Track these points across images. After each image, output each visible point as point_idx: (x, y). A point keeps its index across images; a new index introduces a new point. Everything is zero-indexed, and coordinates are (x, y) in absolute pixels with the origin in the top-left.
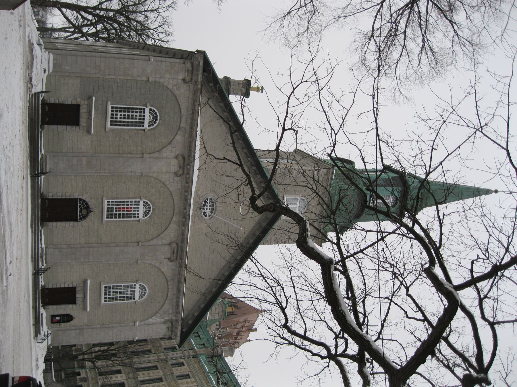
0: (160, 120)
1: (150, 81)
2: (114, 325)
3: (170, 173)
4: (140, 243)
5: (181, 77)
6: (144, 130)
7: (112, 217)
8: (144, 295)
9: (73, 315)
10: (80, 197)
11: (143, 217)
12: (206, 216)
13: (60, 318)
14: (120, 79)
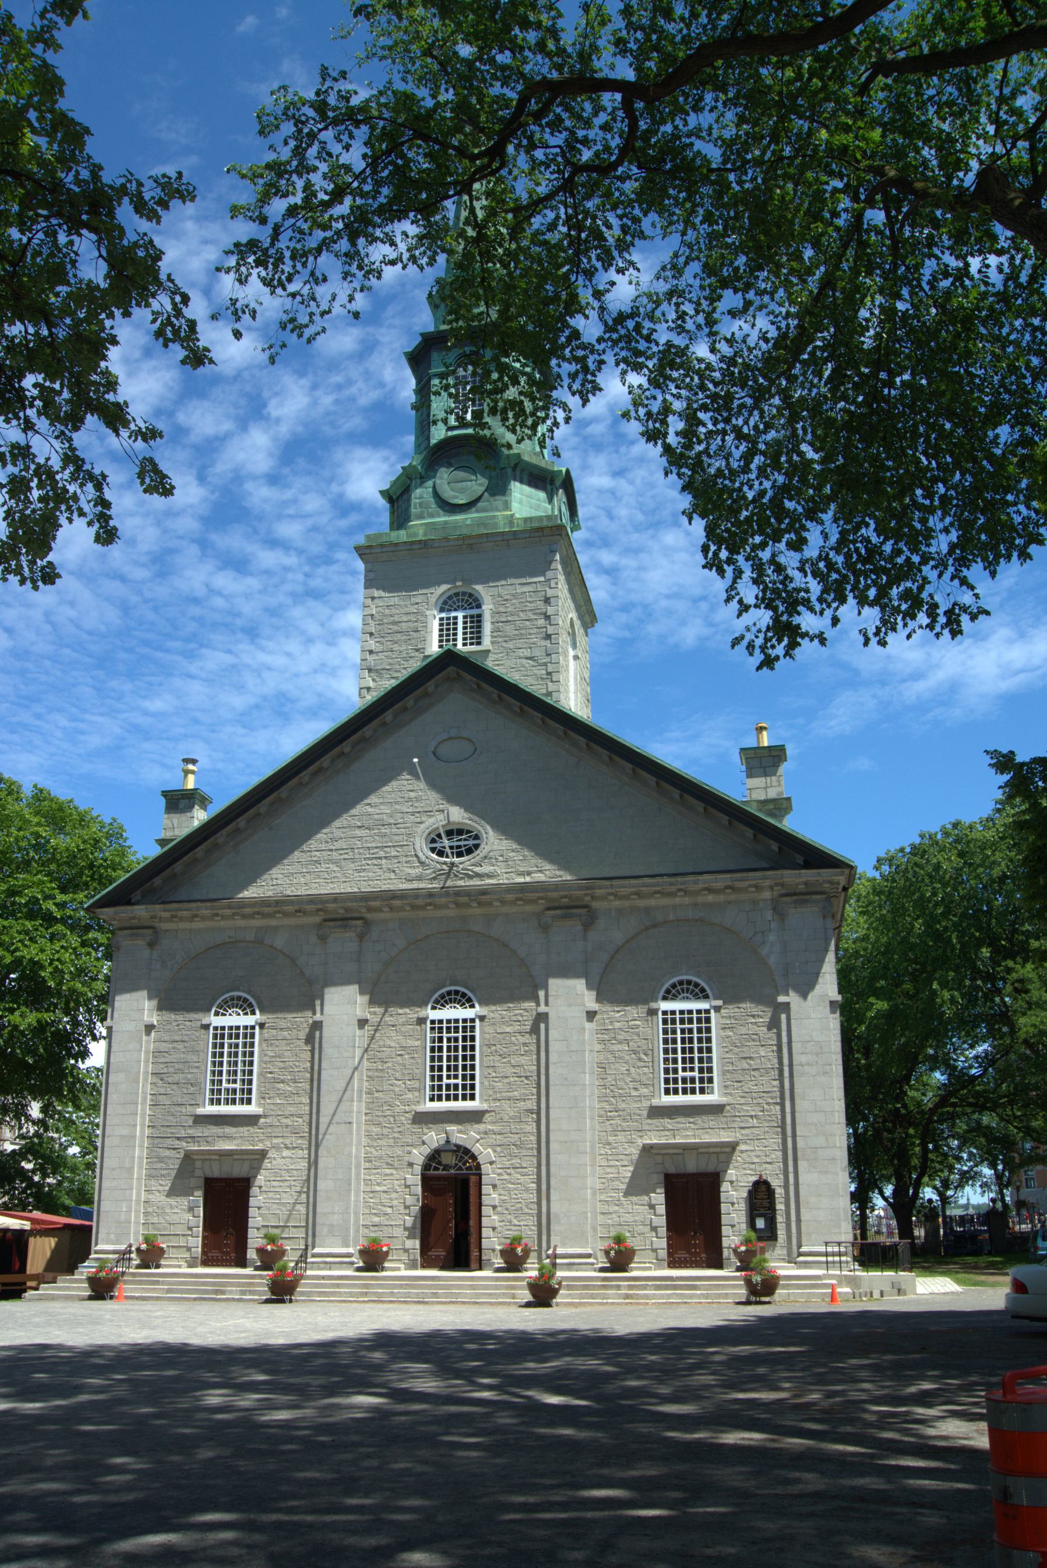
0: (239, 990)
3: (360, 952)
5: (147, 952)
7: (473, 1087)
8: (697, 985)
9: (755, 1178)
10: (418, 1169)
13: (760, 1215)
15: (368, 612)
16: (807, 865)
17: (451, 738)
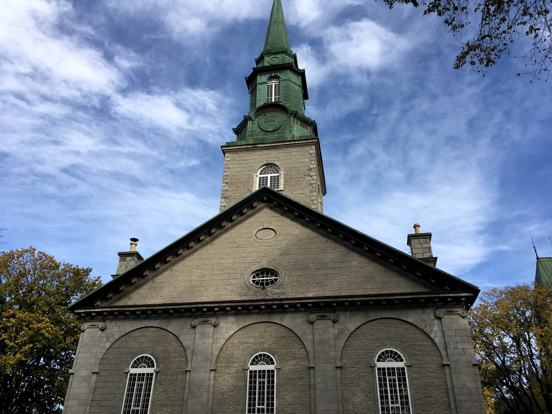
0: (147, 353)
1: (97, 370)
2: (452, 399)
4: (312, 365)
6: (157, 373)
8: (396, 353)
11: (273, 363)
12: (276, 280)
14: (90, 410)
15: (225, 174)
16: (453, 290)
17: (264, 229)
